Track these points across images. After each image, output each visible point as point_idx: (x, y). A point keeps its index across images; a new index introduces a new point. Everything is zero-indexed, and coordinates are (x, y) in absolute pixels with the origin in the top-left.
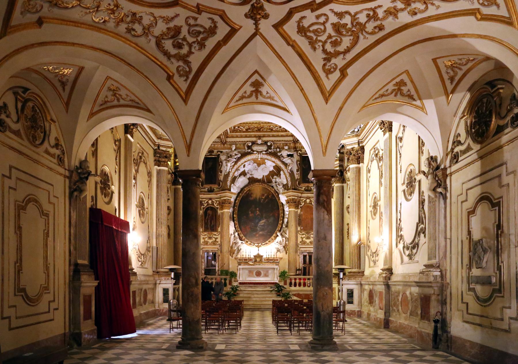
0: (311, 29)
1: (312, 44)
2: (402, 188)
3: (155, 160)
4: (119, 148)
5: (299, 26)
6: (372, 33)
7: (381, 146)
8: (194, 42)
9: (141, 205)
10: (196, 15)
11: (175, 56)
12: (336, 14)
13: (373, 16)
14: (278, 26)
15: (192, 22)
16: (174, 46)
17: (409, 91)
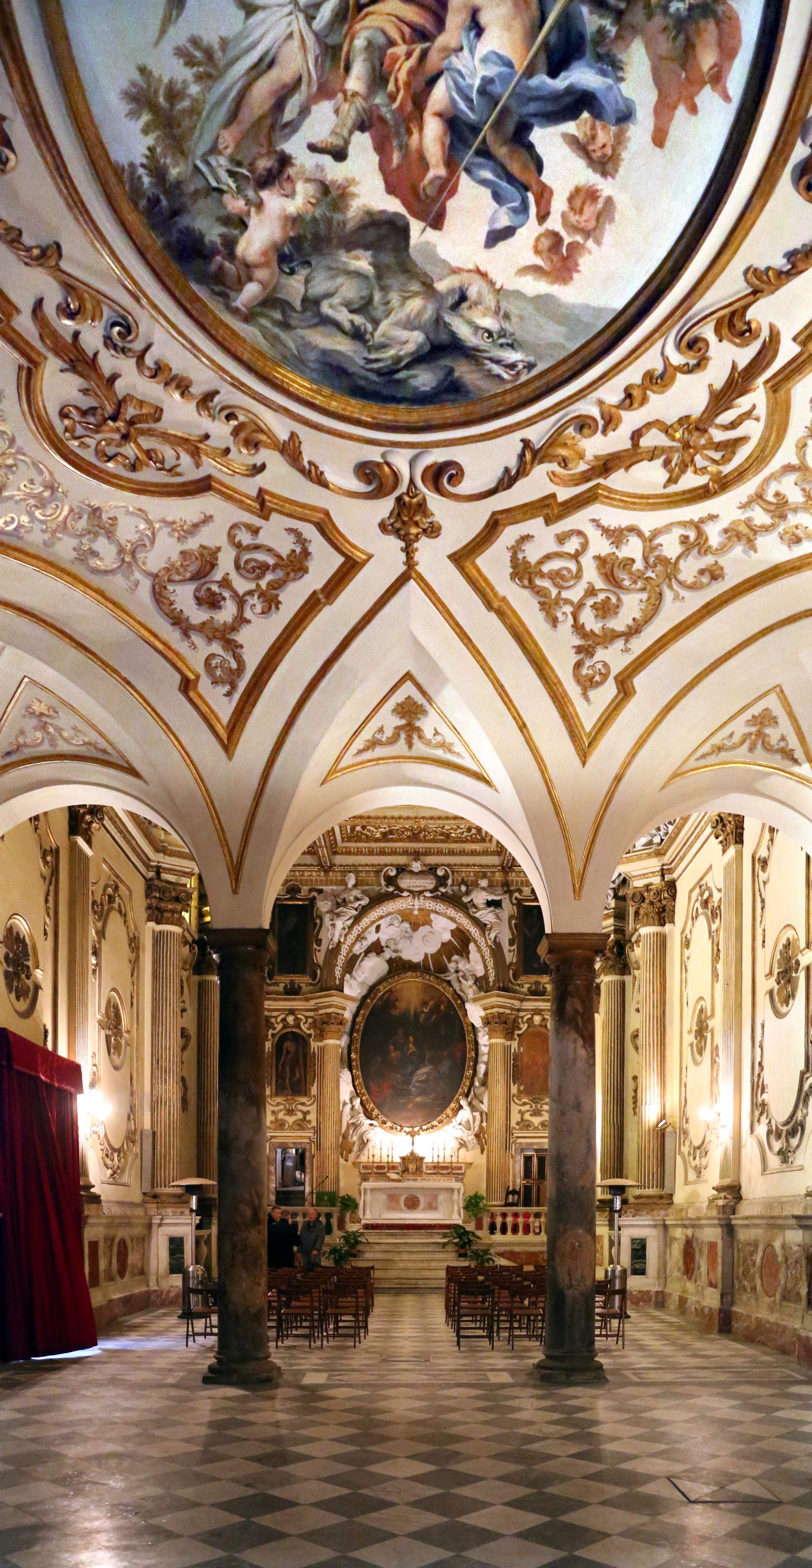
0: (546, 568)
1: (548, 607)
2: (766, 984)
3: (149, 907)
4: (55, 871)
5: (514, 559)
6: (693, 587)
7: (716, 880)
8: (250, 593)
9: (112, 1022)
10: (256, 521)
11: (202, 628)
12: (606, 532)
13: (696, 543)
14: (461, 558)
15: (245, 538)
16: (199, 601)
17: (783, 738)
